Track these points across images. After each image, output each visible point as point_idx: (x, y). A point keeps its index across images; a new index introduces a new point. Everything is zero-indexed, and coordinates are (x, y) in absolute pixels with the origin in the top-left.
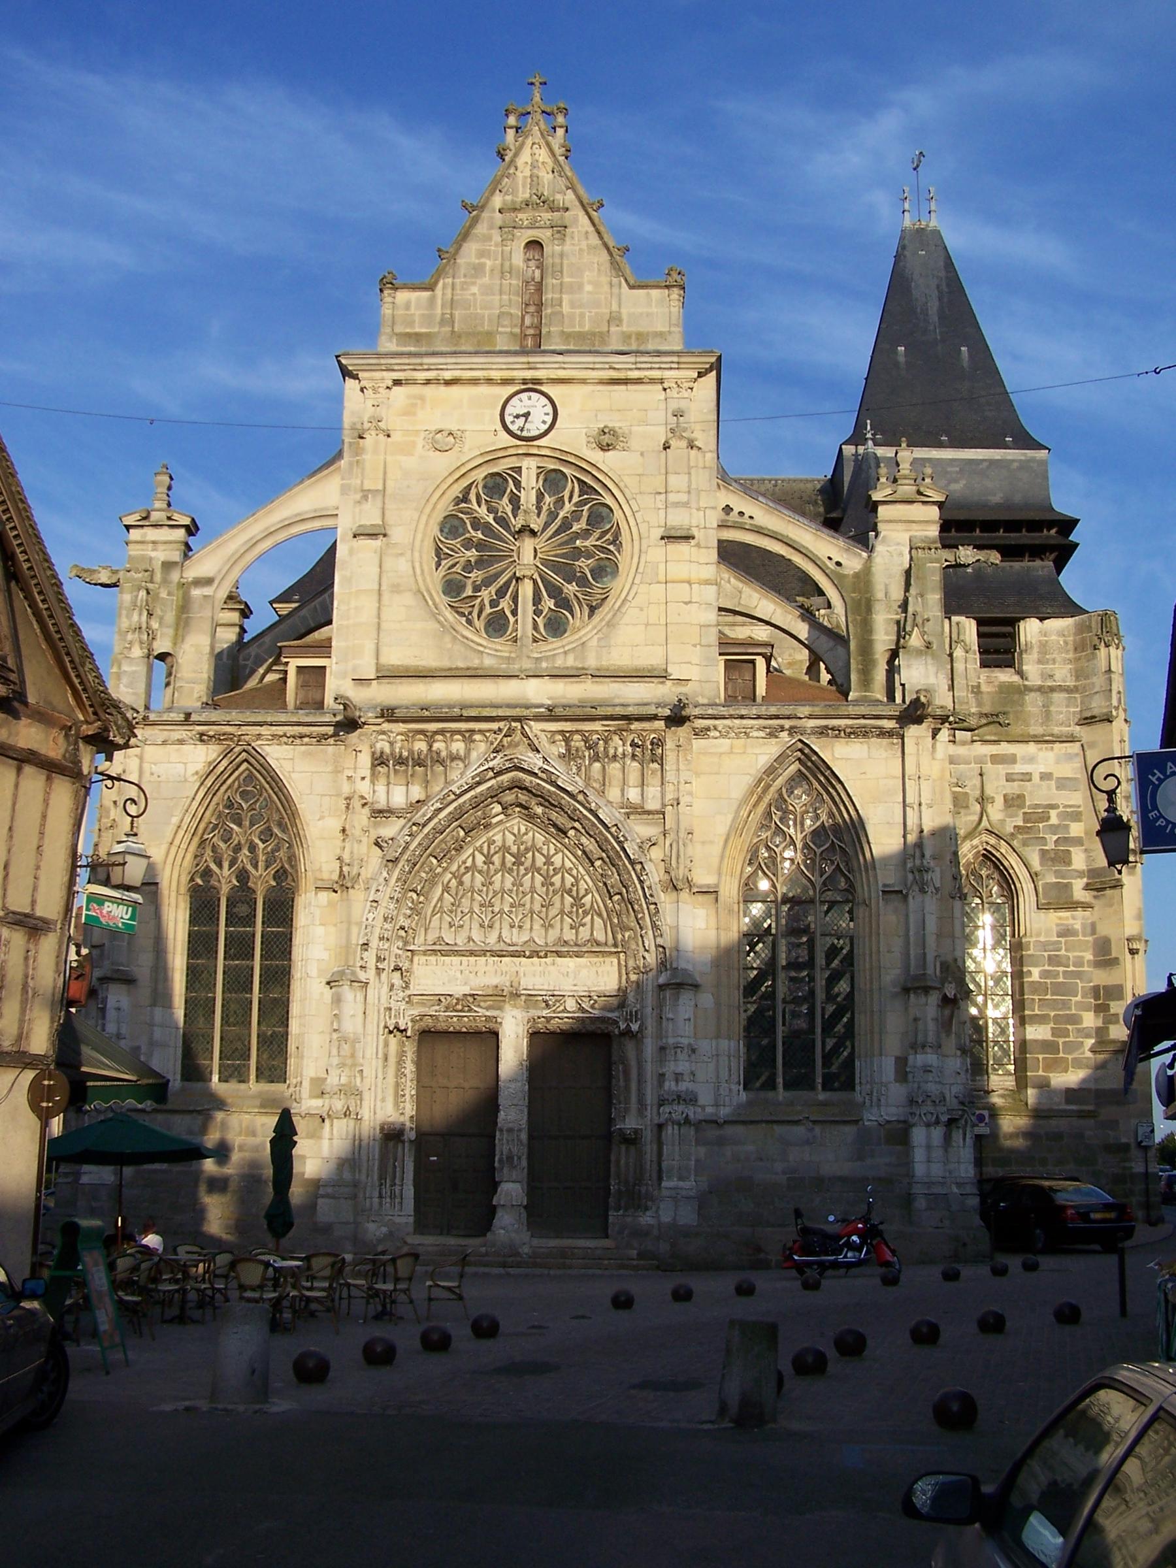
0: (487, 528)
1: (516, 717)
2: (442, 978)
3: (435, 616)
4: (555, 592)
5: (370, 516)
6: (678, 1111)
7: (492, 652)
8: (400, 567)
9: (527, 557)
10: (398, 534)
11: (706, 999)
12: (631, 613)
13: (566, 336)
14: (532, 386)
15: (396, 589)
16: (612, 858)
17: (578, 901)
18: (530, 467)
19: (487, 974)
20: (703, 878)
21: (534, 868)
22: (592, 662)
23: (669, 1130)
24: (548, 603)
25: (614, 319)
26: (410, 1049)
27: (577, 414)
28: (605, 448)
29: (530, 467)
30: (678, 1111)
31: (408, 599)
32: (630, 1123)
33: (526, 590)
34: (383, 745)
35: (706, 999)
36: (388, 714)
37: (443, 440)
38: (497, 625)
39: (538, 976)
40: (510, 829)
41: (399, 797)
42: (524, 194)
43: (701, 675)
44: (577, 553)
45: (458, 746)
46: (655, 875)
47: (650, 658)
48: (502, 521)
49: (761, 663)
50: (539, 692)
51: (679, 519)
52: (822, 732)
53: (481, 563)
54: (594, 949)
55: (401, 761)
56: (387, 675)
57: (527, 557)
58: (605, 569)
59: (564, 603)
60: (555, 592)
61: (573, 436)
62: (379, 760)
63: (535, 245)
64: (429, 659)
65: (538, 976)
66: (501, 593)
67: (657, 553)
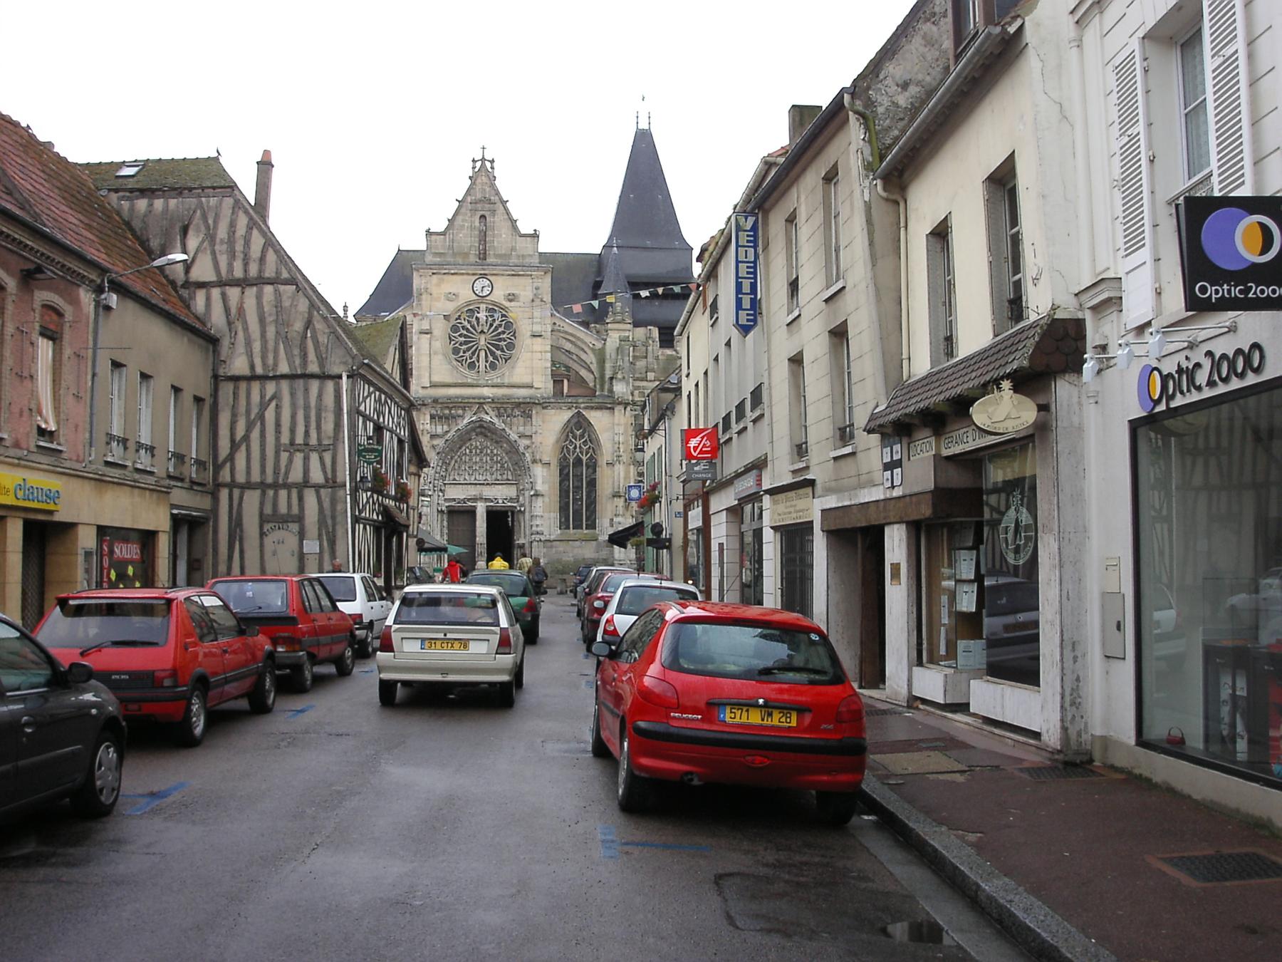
0: (468, 330)
1: (481, 403)
2: (457, 493)
3: (450, 363)
4: (493, 354)
5: (426, 326)
6: (538, 537)
7: (470, 376)
8: (437, 345)
9: (482, 342)
10: (436, 332)
11: (547, 499)
12: (520, 363)
13: (497, 256)
14: (484, 276)
15: (436, 353)
16: (513, 450)
17: (502, 466)
18: (483, 306)
19: (472, 491)
20: (546, 459)
21: (487, 454)
22: (506, 381)
23: (535, 544)
24: (491, 359)
25: (513, 249)
26: (445, 517)
27: (500, 289)
28: (511, 301)
29: (483, 306)
30: (538, 537)
31: (440, 357)
32: (521, 541)
33: (482, 354)
34: (433, 412)
35: (547, 499)
36: (436, 401)
37: (451, 297)
38: (472, 366)
39: (488, 492)
40: (477, 442)
41: (439, 430)
42: (479, 196)
43: (544, 385)
44: (500, 340)
45: (460, 412)
46: (528, 457)
47: (526, 379)
48: (473, 327)
49: (566, 382)
50: (487, 392)
51: (537, 328)
52: (586, 408)
53: (466, 342)
54: (508, 483)
55: (440, 418)
56: (433, 385)
57: (482, 342)
58: (511, 346)
59: (496, 358)
60: (493, 354)
61: (498, 296)
62: (432, 417)
63: (483, 217)
64: (448, 380)
65: (488, 492)
66: (473, 354)
67: (528, 341)
